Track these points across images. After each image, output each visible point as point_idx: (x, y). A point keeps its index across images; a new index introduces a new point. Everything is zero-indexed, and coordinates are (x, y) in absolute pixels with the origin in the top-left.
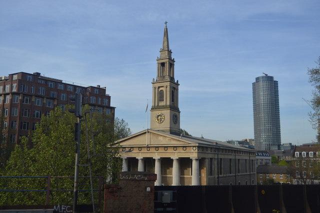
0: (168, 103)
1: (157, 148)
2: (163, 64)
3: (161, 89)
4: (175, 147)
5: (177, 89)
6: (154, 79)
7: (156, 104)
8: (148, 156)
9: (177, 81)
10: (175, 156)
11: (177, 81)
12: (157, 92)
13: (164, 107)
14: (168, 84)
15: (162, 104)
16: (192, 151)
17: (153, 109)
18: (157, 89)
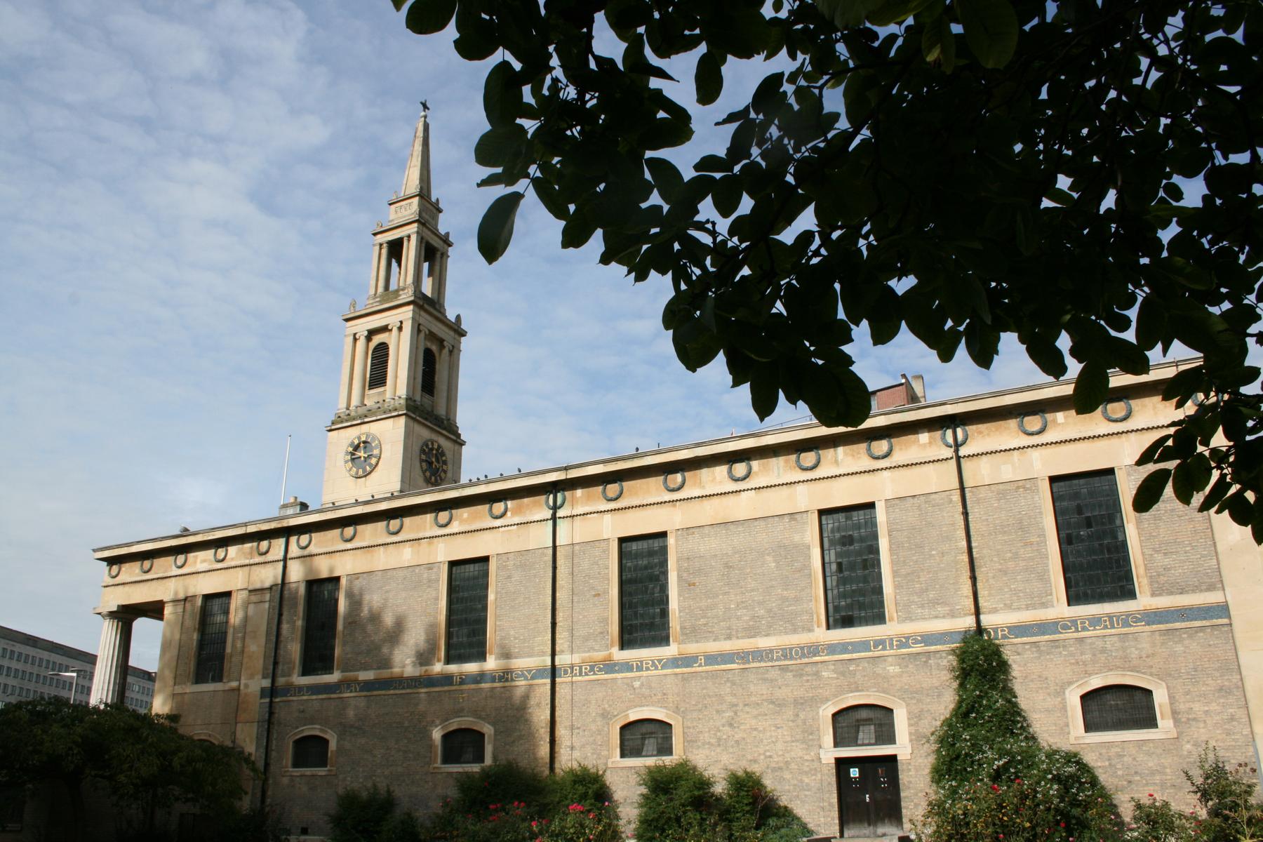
0: (402, 391)
2: (395, 249)
3: (377, 339)
5: (454, 351)
6: (354, 305)
7: (355, 401)
9: (458, 317)
11: (458, 317)
13: (383, 413)
14: (407, 313)
18: (361, 343)
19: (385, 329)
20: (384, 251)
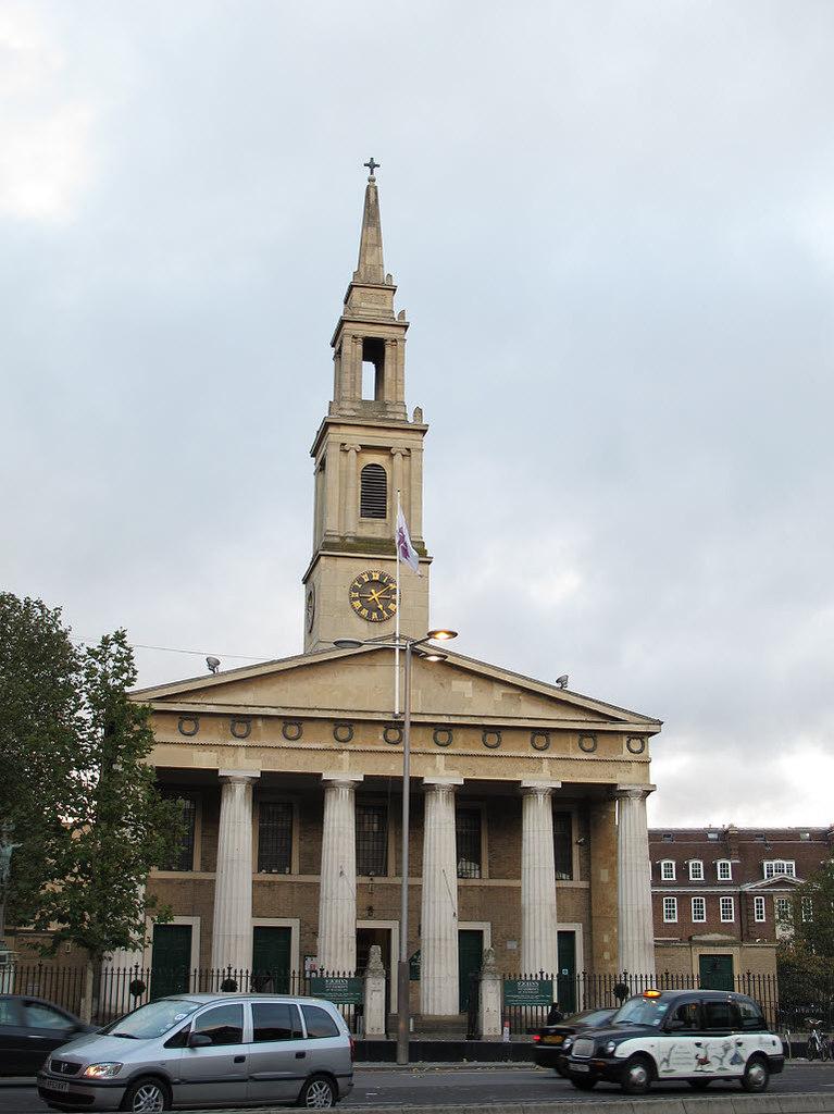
1: (444, 731)
4: (541, 735)
8: (389, 768)
10: (542, 776)
12: (353, 469)
15: (374, 529)
16: (626, 755)
17: (328, 547)
19: (386, 450)
20: (360, 347)
